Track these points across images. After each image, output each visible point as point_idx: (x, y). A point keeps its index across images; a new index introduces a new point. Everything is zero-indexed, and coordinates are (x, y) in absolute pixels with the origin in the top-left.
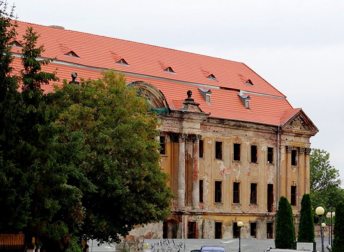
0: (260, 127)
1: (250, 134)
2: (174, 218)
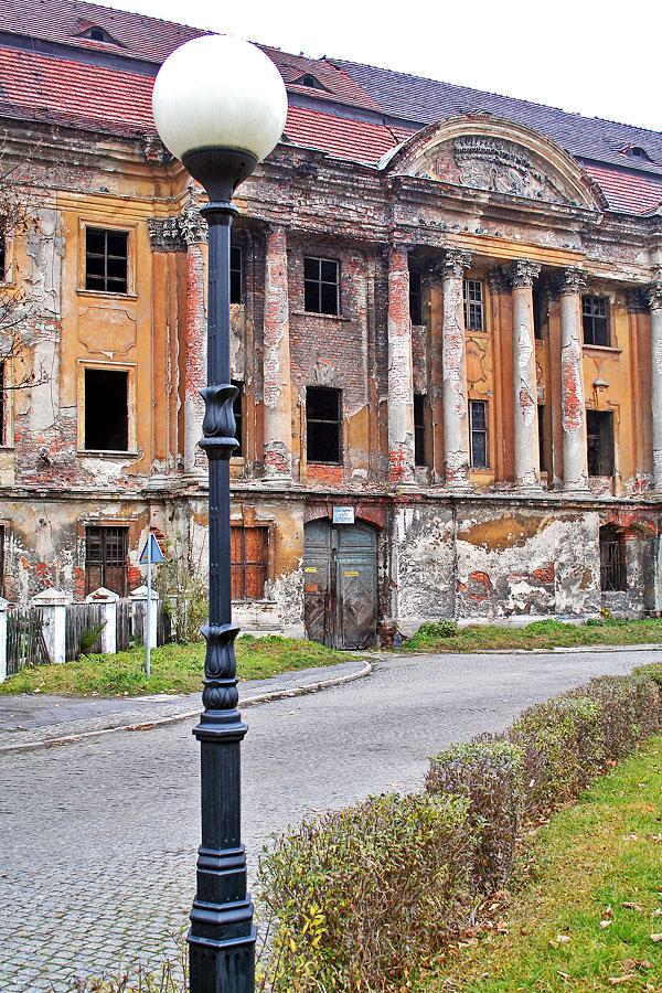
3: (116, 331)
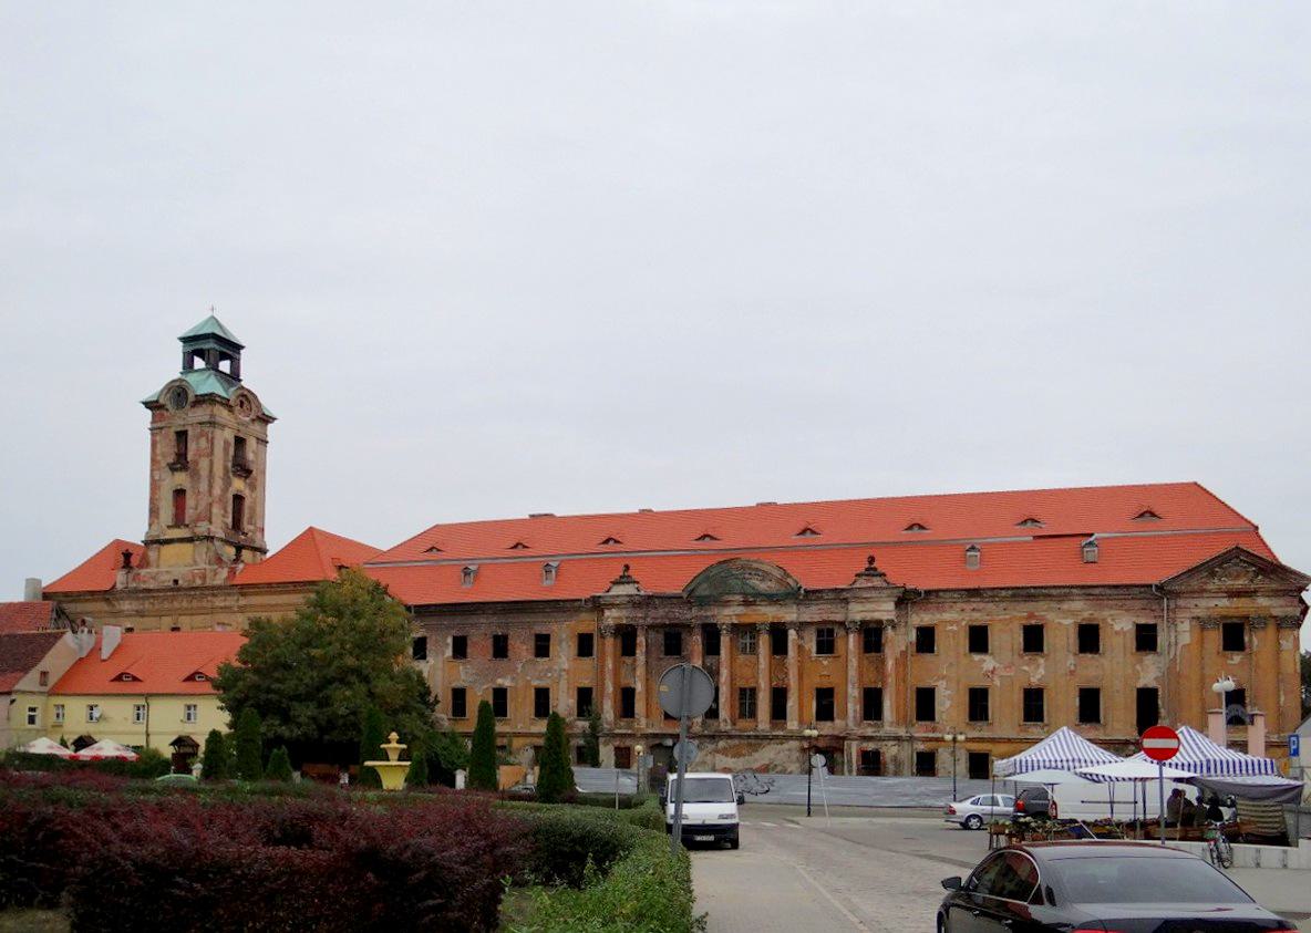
0: (1097, 591)
1: (1078, 605)
2: (835, 745)
3: (585, 671)
